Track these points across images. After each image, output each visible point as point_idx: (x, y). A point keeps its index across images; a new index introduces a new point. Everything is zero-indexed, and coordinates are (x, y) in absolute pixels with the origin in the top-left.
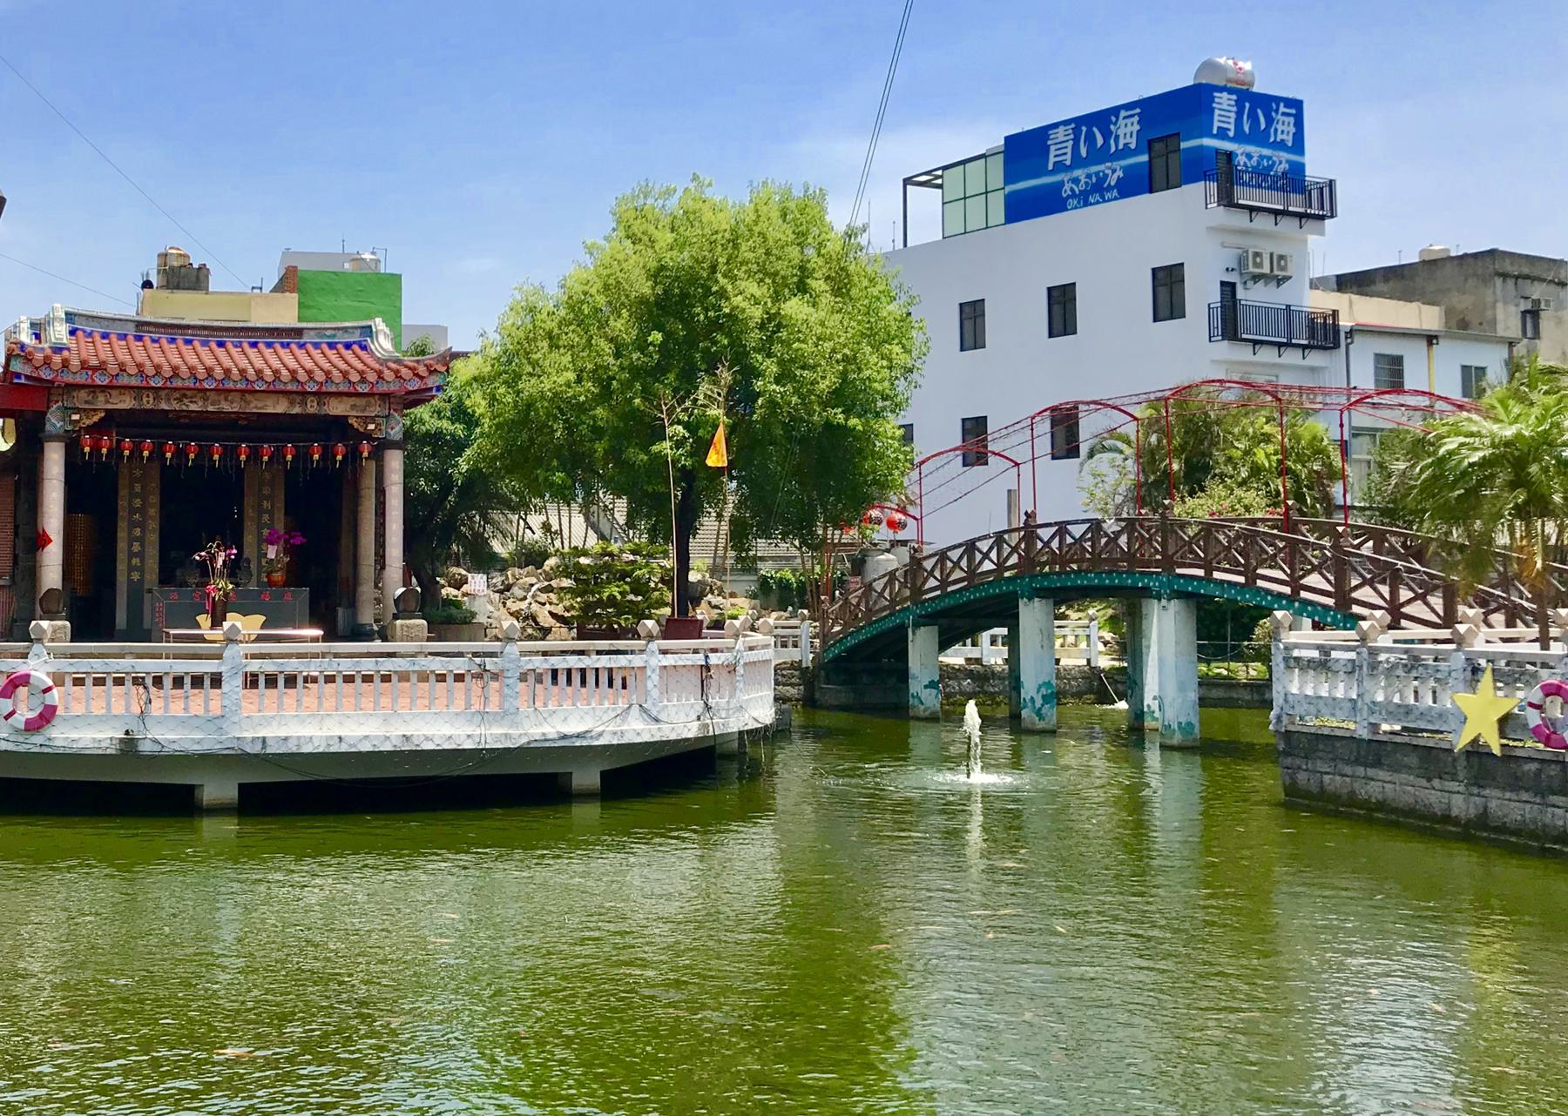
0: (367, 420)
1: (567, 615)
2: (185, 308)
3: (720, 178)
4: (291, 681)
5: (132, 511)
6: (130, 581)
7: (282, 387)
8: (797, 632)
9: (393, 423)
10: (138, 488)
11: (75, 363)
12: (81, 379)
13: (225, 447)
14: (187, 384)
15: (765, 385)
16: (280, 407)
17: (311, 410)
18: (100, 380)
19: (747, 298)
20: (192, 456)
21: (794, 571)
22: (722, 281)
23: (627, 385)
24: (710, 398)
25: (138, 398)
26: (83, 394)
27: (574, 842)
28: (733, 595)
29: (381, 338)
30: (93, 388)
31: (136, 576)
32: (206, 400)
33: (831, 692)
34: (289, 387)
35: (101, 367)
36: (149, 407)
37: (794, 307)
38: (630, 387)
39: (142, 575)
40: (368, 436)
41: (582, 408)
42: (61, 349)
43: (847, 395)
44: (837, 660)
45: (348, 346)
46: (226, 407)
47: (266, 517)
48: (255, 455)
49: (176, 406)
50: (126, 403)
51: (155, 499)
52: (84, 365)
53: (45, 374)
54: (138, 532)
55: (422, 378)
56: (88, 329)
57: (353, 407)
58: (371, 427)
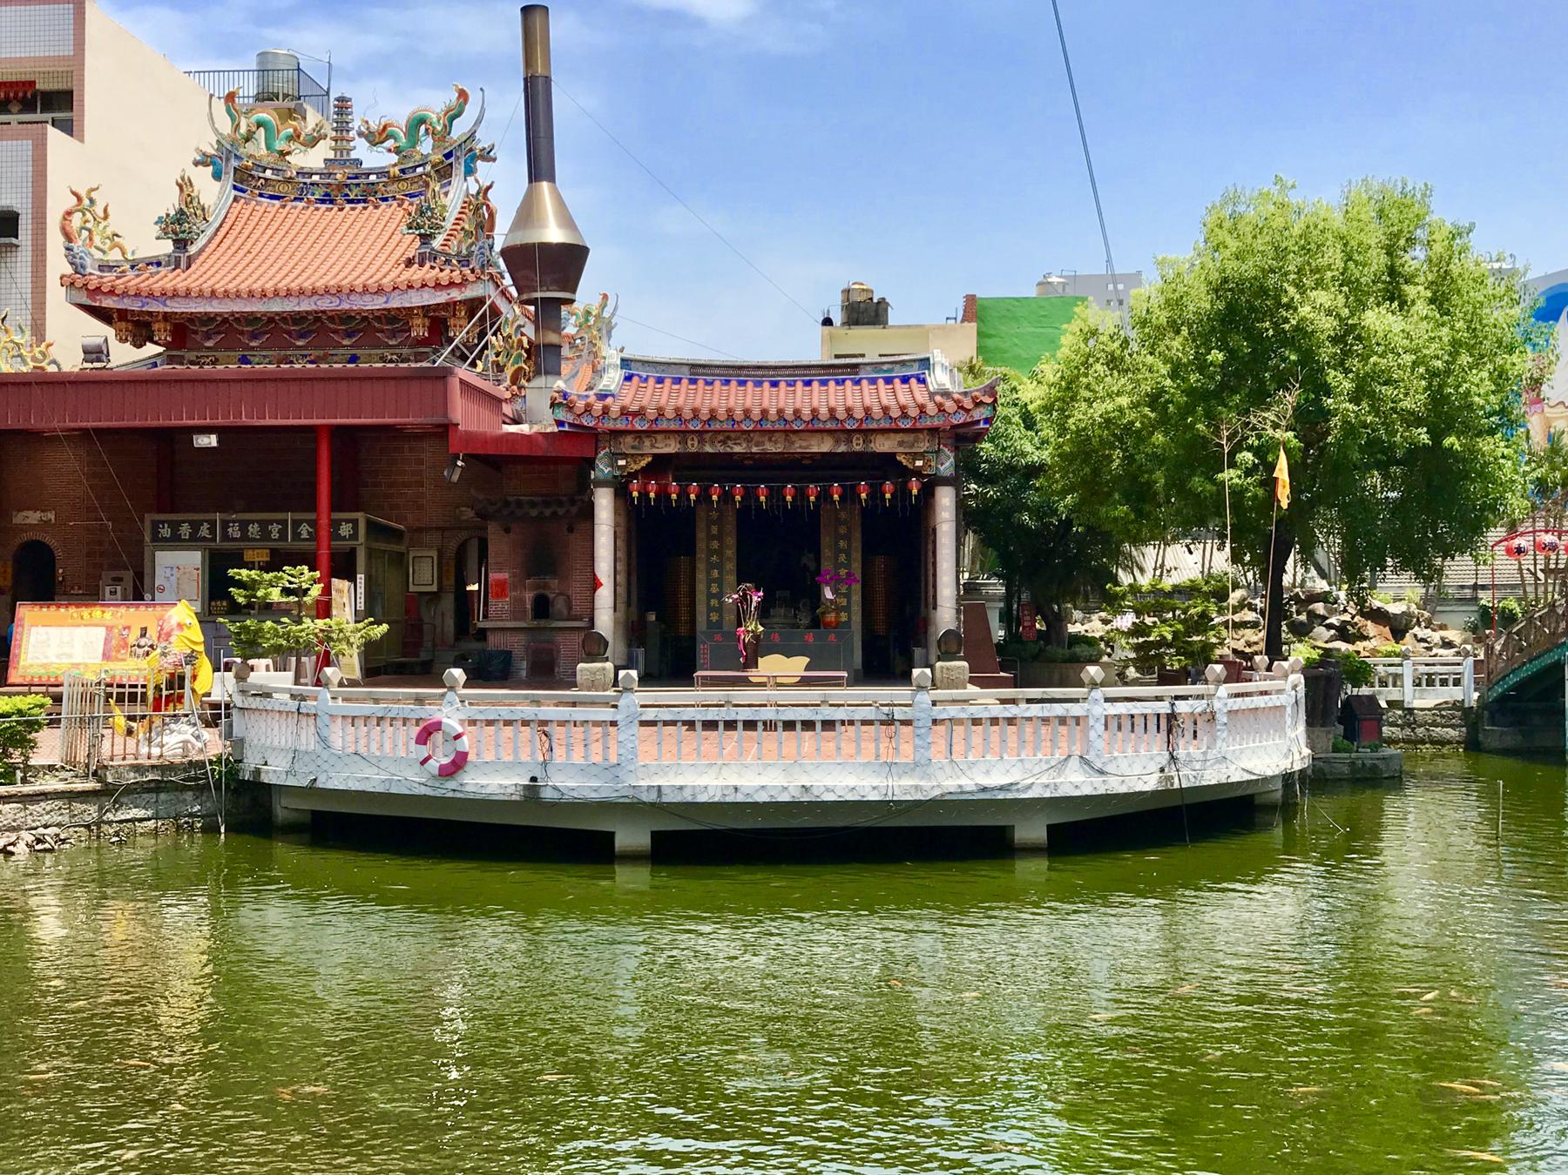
0: (916, 456)
1: (1247, 650)
2: (867, 344)
3: (1316, 180)
4: (828, 725)
5: (710, 552)
6: (709, 621)
7: (821, 426)
8: (1398, 670)
9: (943, 457)
10: (714, 530)
11: (615, 409)
12: (621, 425)
13: (770, 489)
14: (725, 427)
15: (1341, 406)
16: (824, 446)
17: (858, 448)
18: (638, 425)
19: (1317, 309)
20: (738, 498)
21: (1519, 600)
22: (1292, 290)
23: (1188, 410)
24: (1275, 423)
25: (684, 442)
26: (629, 439)
27: (1013, 896)
28: (1443, 627)
29: (938, 370)
30: (639, 434)
31: (714, 617)
32: (749, 441)
33: (1493, 734)
34: (829, 426)
35: (640, 413)
36: (693, 450)
37: (1378, 319)
38: (1192, 412)
39: (721, 616)
40: (917, 473)
41: (1141, 437)
42: (606, 396)
43: (1445, 412)
44: (1503, 699)
45: (905, 380)
46: (770, 448)
47: (842, 557)
48: (704, 496)
49: (721, 449)
50: (671, 447)
51: (731, 541)
52: (624, 412)
53: (587, 421)
54: (715, 573)
55: (968, 411)
56: (644, 375)
57: (901, 444)
58: (919, 463)
